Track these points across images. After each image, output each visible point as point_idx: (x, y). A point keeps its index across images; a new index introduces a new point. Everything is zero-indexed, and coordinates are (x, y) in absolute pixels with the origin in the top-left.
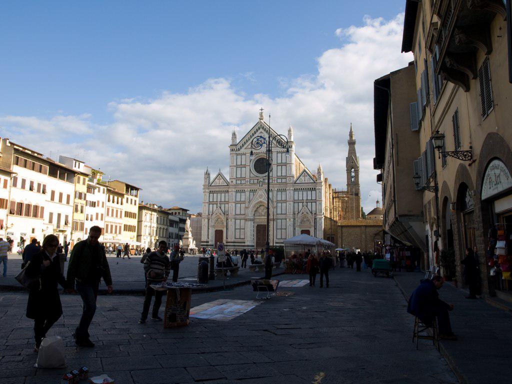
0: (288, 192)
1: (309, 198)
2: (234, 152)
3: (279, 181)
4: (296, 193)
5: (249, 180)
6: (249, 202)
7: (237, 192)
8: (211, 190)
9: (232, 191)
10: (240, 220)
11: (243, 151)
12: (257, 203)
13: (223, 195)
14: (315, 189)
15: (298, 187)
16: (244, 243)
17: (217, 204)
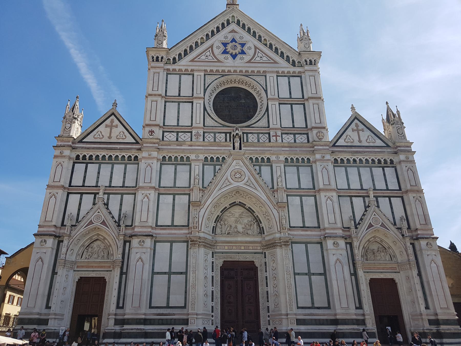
0: (318, 167)
1: (380, 185)
2: (161, 64)
3: (289, 139)
4: (341, 171)
5: (201, 132)
6: (203, 189)
7: (164, 161)
8: (82, 153)
9: (150, 157)
10: (172, 242)
11: (184, 63)
12: (225, 196)
13: (119, 169)
14: (392, 162)
15: (345, 157)
16: (186, 322)
17: (95, 194)
